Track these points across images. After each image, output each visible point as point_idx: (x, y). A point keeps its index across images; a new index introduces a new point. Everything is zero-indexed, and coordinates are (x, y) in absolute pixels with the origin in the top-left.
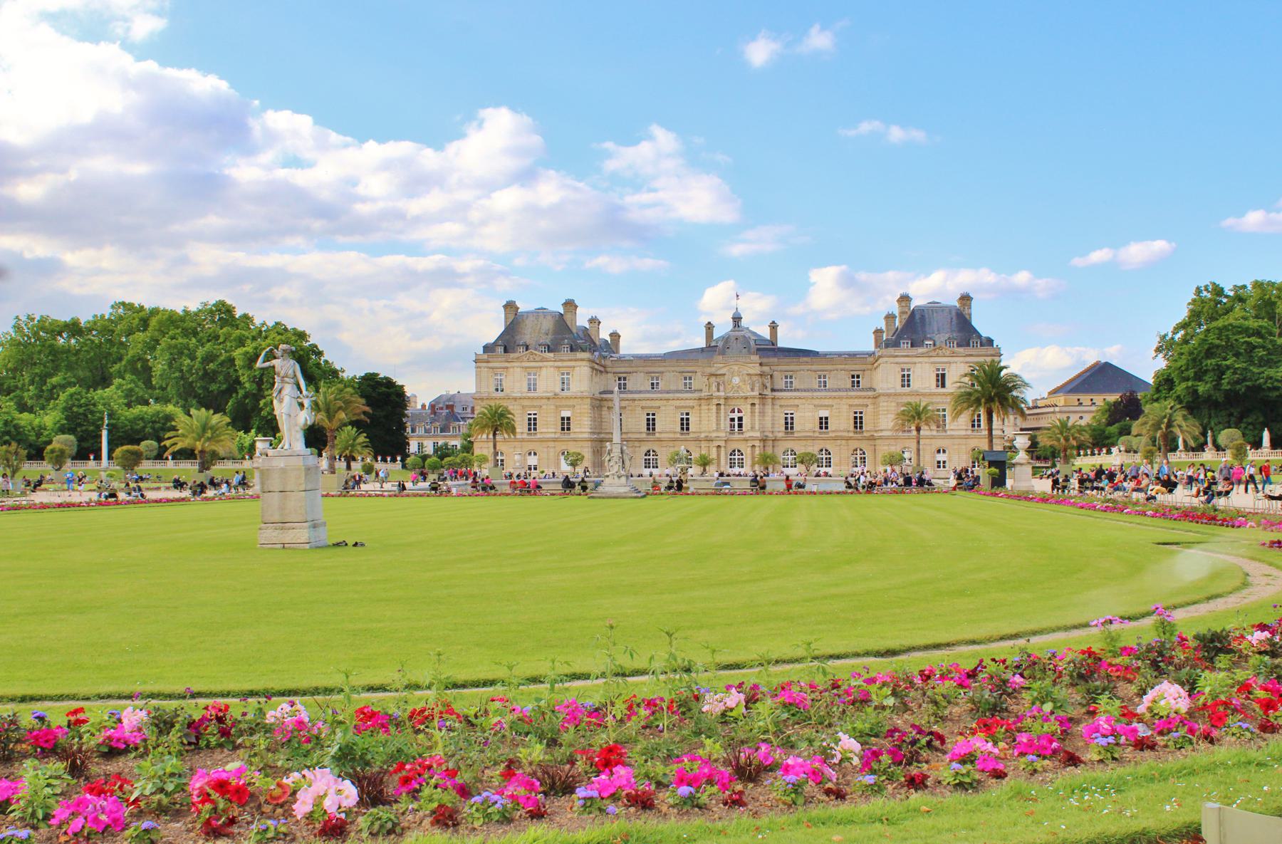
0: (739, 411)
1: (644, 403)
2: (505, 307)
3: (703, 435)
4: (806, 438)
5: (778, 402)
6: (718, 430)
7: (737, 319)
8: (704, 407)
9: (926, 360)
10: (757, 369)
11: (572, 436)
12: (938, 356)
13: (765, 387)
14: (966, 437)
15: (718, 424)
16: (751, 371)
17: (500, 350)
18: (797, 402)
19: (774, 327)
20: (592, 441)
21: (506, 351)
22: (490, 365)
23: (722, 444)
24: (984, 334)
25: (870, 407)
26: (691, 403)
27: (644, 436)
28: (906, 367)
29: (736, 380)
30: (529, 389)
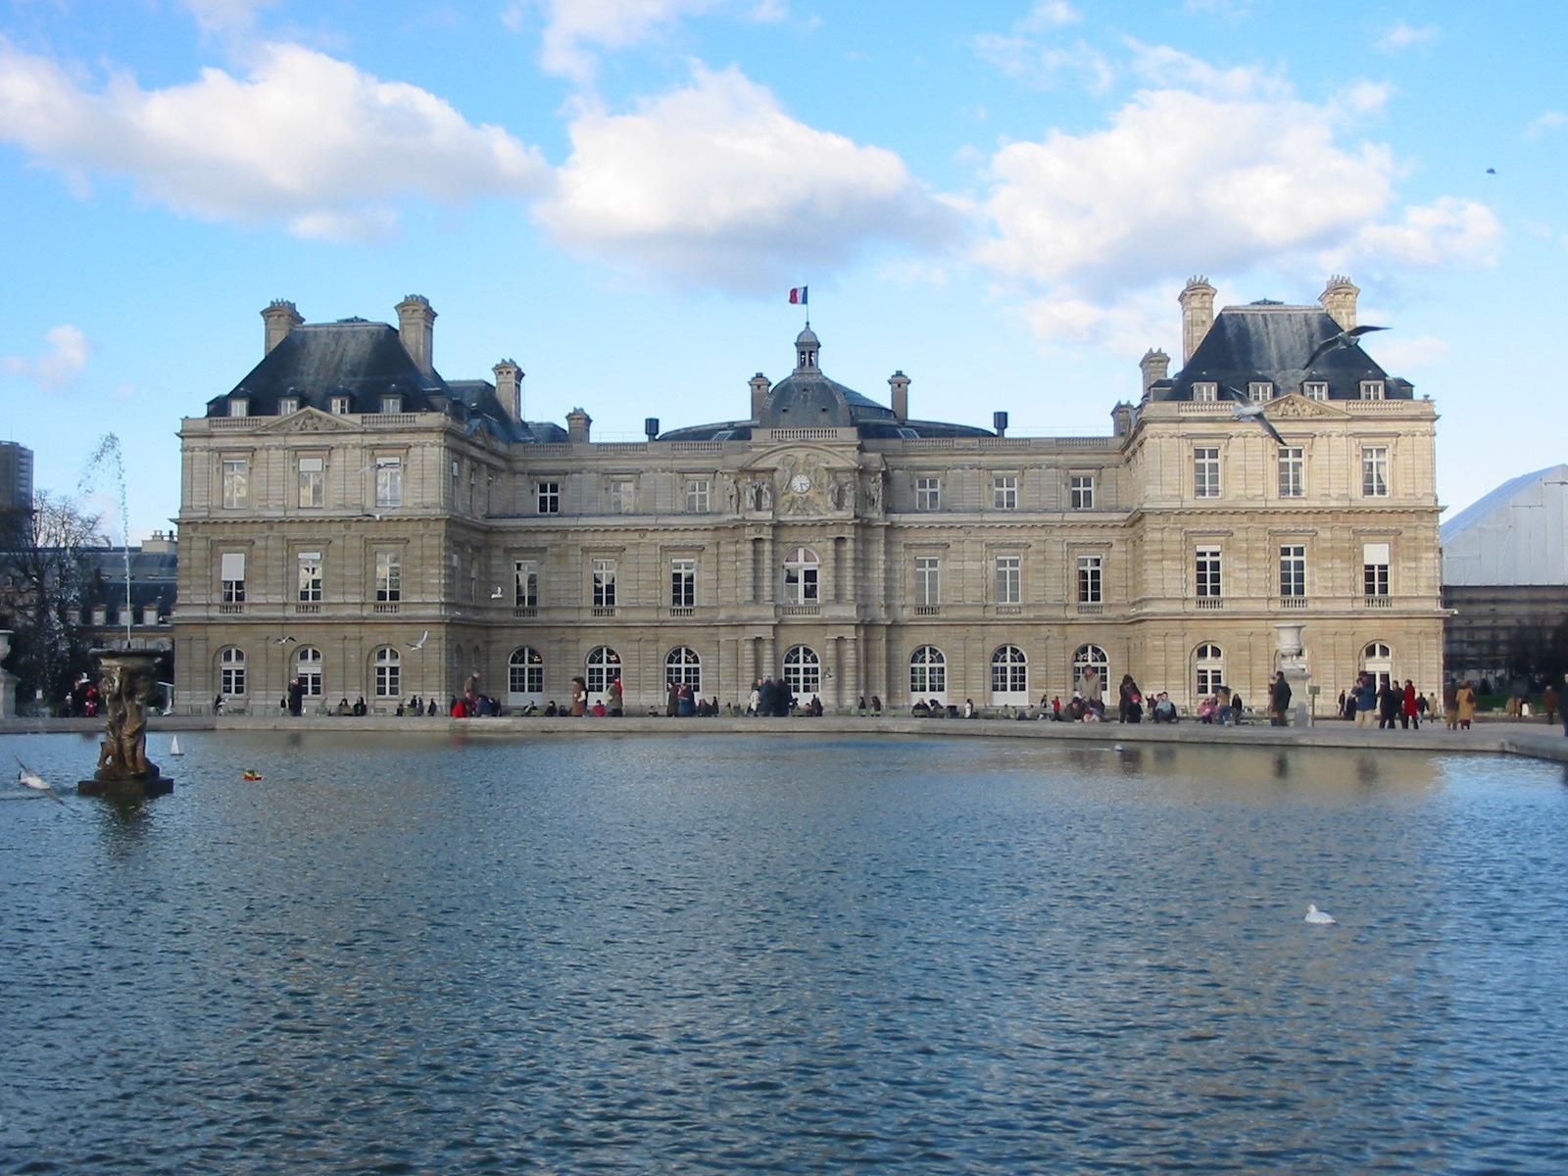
1: (588, 540)
2: (267, 314)
3: (723, 615)
4: (965, 623)
5: (900, 537)
6: (756, 598)
8: (722, 550)
10: (848, 459)
14: (1355, 617)
16: (838, 463)
17: (239, 408)
18: (944, 536)
20: (452, 624)
21: (254, 410)
22: (215, 443)
23: (767, 633)
24: (1392, 373)
25: (1118, 553)
28: (1206, 444)
29: (800, 483)
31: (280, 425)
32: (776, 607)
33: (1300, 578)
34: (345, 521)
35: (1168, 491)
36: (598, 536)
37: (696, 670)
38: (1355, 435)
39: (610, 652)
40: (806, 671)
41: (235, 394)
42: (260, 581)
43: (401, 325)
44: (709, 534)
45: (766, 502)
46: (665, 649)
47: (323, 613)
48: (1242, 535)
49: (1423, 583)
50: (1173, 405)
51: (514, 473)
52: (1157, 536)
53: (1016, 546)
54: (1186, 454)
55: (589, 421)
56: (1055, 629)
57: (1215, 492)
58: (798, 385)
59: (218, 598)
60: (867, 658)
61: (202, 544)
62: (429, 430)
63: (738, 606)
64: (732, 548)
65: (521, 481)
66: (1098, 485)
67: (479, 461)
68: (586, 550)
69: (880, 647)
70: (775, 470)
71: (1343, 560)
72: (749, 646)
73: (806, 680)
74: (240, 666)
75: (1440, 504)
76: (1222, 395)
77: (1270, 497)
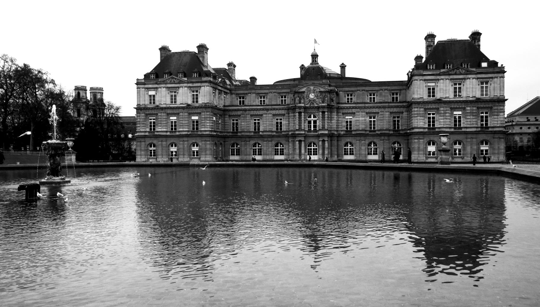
0: (314, 117)
1: (252, 113)
3: (290, 133)
5: (341, 111)
7: (315, 57)
9: (447, 77)
11: (199, 133)
12: (456, 74)
13: (332, 100)
15: (300, 125)
16: (322, 90)
19: (343, 67)
22: (146, 86)
23: (303, 139)
24: (491, 59)
25: (405, 114)
26: (283, 112)
27: (252, 134)
29: (312, 96)
30: (172, 102)
31: (164, 81)
32: (305, 131)
33: (460, 121)
34: (183, 108)
35: (419, 96)
36: (255, 111)
37: (283, 149)
38: (478, 78)
39: (259, 144)
40: (314, 149)
41: (151, 73)
42: (160, 125)
43: (198, 52)
44: (286, 111)
45: (302, 101)
46: (274, 143)
47: (177, 133)
48: (442, 109)
49: (499, 122)
50: (422, 71)
51: (232, 94)
52: (416, 109)
53: (375, 113)
54: (425, 85)
55: (256, 79)
56: (386, 138)
57: (434, 96)
58: (311, 67)
59: (148, 130)
60: (331, 145)
61: (143, 115)
62: (206, 82)
63: (294, 131)
64: (293, 115)
65: (234, 96)
66: (400, 95)
67: (221, 91)
68: (252, 116)
69: (335, 142)
70: (304, 92)
71: (473, 116)
72: (297, 142)
73: (314, 152)
74: (155, 148)
75: (506, 98)
76: (437, 68)
77: (450, 97)
